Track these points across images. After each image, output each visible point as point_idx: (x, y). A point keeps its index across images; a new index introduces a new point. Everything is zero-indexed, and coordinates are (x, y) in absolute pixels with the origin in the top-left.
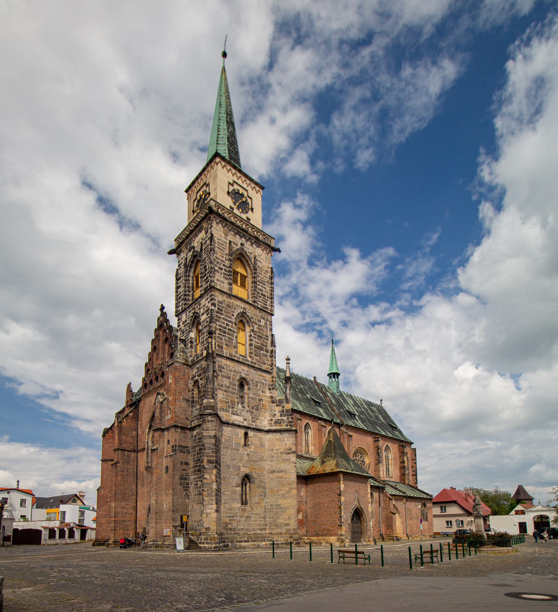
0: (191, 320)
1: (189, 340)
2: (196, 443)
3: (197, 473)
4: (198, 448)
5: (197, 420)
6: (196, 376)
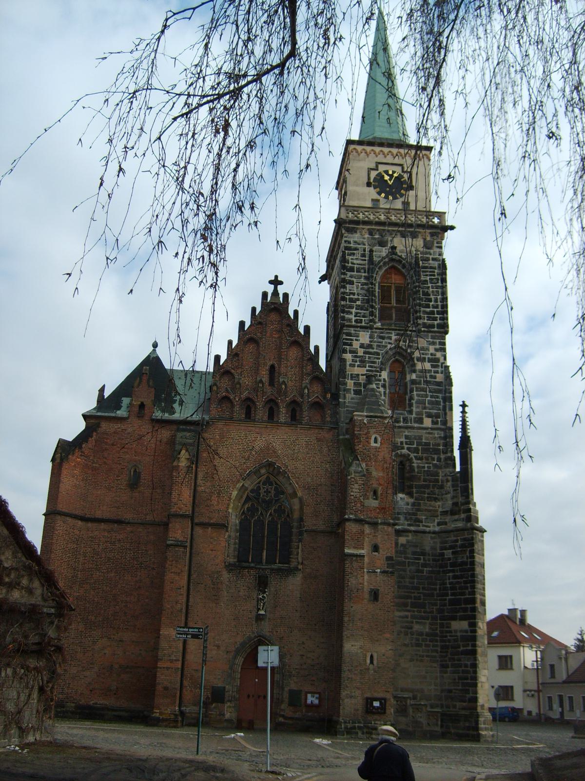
0: (387, 352)
1: (380, 380)
3: (409, 608)
4: (413, 568)
6: (403, 448)
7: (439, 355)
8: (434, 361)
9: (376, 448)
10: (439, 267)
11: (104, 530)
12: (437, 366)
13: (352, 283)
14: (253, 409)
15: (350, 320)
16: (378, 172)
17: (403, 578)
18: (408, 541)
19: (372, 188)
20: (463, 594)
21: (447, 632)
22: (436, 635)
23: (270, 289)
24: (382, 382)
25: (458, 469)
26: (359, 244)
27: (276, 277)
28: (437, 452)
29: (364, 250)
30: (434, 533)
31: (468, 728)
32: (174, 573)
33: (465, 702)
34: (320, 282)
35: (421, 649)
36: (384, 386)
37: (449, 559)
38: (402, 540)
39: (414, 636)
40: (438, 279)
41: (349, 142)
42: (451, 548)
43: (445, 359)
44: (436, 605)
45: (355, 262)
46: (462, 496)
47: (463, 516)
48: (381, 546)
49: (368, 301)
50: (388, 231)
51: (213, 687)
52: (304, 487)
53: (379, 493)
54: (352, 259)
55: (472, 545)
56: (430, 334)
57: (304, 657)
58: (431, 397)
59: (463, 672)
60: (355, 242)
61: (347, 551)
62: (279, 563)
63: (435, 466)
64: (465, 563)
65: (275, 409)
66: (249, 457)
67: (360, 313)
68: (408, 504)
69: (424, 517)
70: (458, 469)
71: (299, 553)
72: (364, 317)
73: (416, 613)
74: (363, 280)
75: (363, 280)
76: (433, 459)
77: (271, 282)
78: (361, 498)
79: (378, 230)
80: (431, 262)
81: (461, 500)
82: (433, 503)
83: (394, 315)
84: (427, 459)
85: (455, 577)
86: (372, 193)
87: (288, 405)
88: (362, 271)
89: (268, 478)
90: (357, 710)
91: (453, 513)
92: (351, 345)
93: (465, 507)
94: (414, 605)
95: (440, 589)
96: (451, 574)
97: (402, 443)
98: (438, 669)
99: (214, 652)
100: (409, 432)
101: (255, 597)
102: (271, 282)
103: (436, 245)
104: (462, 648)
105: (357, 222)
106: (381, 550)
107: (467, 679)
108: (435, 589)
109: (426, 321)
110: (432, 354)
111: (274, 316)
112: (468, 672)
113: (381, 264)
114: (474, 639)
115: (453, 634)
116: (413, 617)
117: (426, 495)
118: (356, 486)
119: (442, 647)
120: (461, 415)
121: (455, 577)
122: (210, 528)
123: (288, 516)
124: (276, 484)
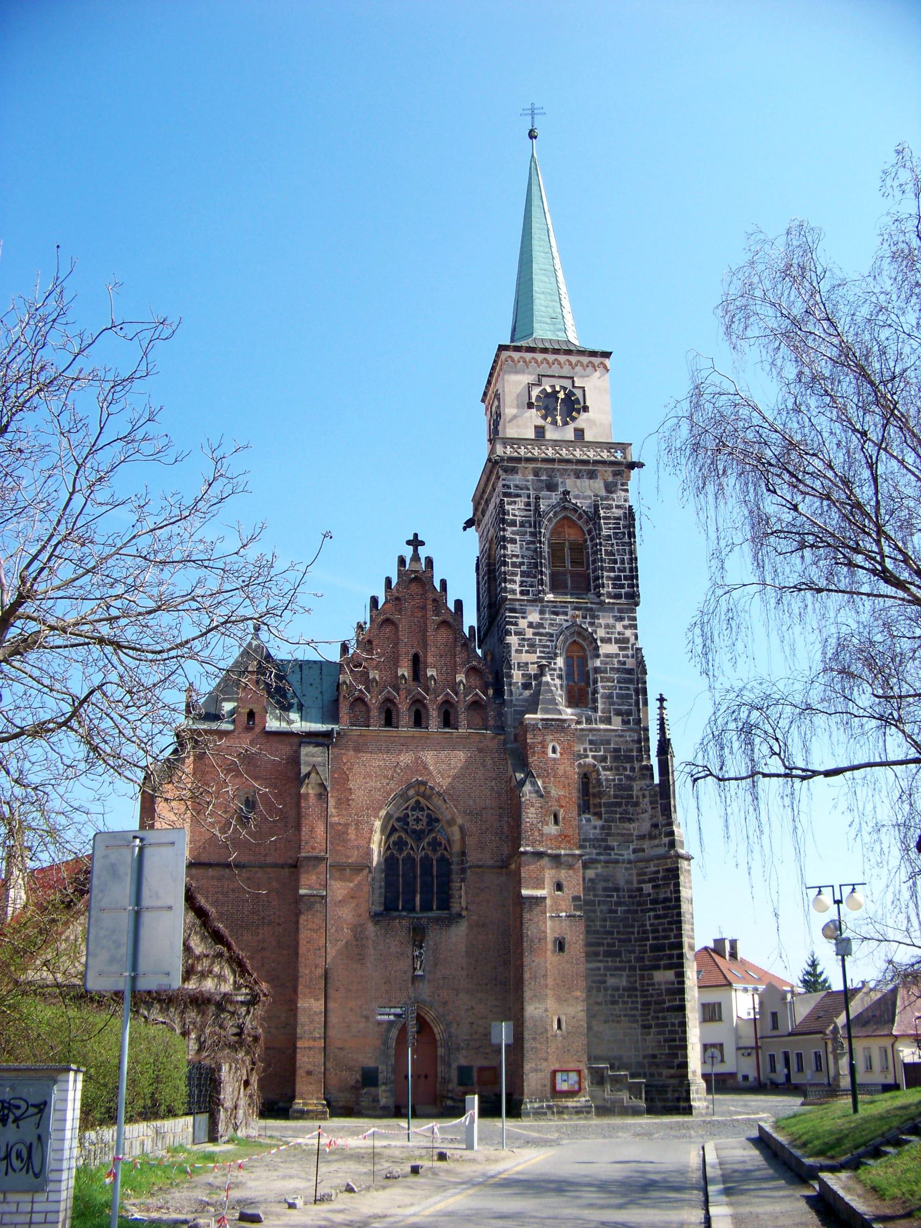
1: (554, 670)
2: (595, 896)
3: (601, 958)
4: (604, 908)
5: (594, 847)
6: (587, 756)
7: (628, 633)
8: (622, 641)
9: (554, 759)
10: (625, 517)
11: (213, 878)
12: (626, 649)
13: (513, 541)
14: (394, 713)
15: (513, 592)
16: (542, 388)
17: (593, 921)
18: (597, 875)
19: (534, 411)
20: (667, 937)
21: (648, 985)
22: (635, 989)
23: (408, 552)
24: (558, 672)
25: (657, 780)
26: (521, 489)
27: (416, 535)
28: (629, 759)
29: (529, 497)
30: (630, 862)
31: (678, 1100)
32: (310, 929)
33: (672, 1068)
34: (465, 529)
35: (616, 1007)
36: (560, 677)
37: (649, 895)
38: (591, 873)
39: (609, 992)
40: (624, 533)
41: (502, 348)
42: (650, 880)
43: (636, 638)
44: (633, 952)
45: (517, 513)
46: (663, 815)
47: (666, 840)
48: (565, 883)
49: (536, 565)
50: (558, 470)
51: (363, 1068)
52: (465, 812)
53: (560, 818)
54: (513, 509)
55: (678, 877)
56: (616, 607)
57: (474, 1026)
58: (621, 688)
59: (671, 1032)
60: (516, 486)
61: (525, 892)
62: (438, 909)
63: (629, 778)
64: (669, 900)
65: (423, 711)
66: (393, 776)
67: (526, 582)
68: (595, 828)
69: (616, 844)
70: (657, 780)
71: (462, 897)
72: (531, 586)
73: (610, 964)
74: (528, 538)
75: (528, 538)
76: (625, 769)
77: (409, 543)
78: (540, 825)
79: (546, 469)
80: (614, 510)
81: (661, 820)
82: (626, 825)
83: (569, 582)
84: (617, 769)
85: (657, 917)
86: (534, 417)
87: (439, 708)
88: (527, 525)
89: (418, 802)
90: (545, 1086)
91: (652, 837)
92: (516, 624)
93: (668, 829)
94: (608, 954)
95: (638, 933)
96: (652, 914)
97: (585, 750)
98: (639, 1031)
99: (362, 1025)
100: (593, 735)
101: (410, 954)
102: (409, 543)
103: (620, 487)
104: (667, 1004)
105: (518, 460)
106: (566, 889)
107: (674, 1040)
108: (633, 933)
109: (610, 589)
110: (619, 633)
111: (415, 588)
112: (675, 1032)
113: (551, 514)
114: (682, 991)
115: (656, 987)
116: (607, 968)
117: (618, 816)
118: (532, 810)
119: (644, 1004)
120: (658, 711)
121: (657, 917)
122: (348, 870)
123: (446, 849)
124: (428, 808)
